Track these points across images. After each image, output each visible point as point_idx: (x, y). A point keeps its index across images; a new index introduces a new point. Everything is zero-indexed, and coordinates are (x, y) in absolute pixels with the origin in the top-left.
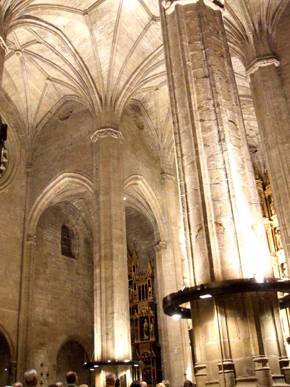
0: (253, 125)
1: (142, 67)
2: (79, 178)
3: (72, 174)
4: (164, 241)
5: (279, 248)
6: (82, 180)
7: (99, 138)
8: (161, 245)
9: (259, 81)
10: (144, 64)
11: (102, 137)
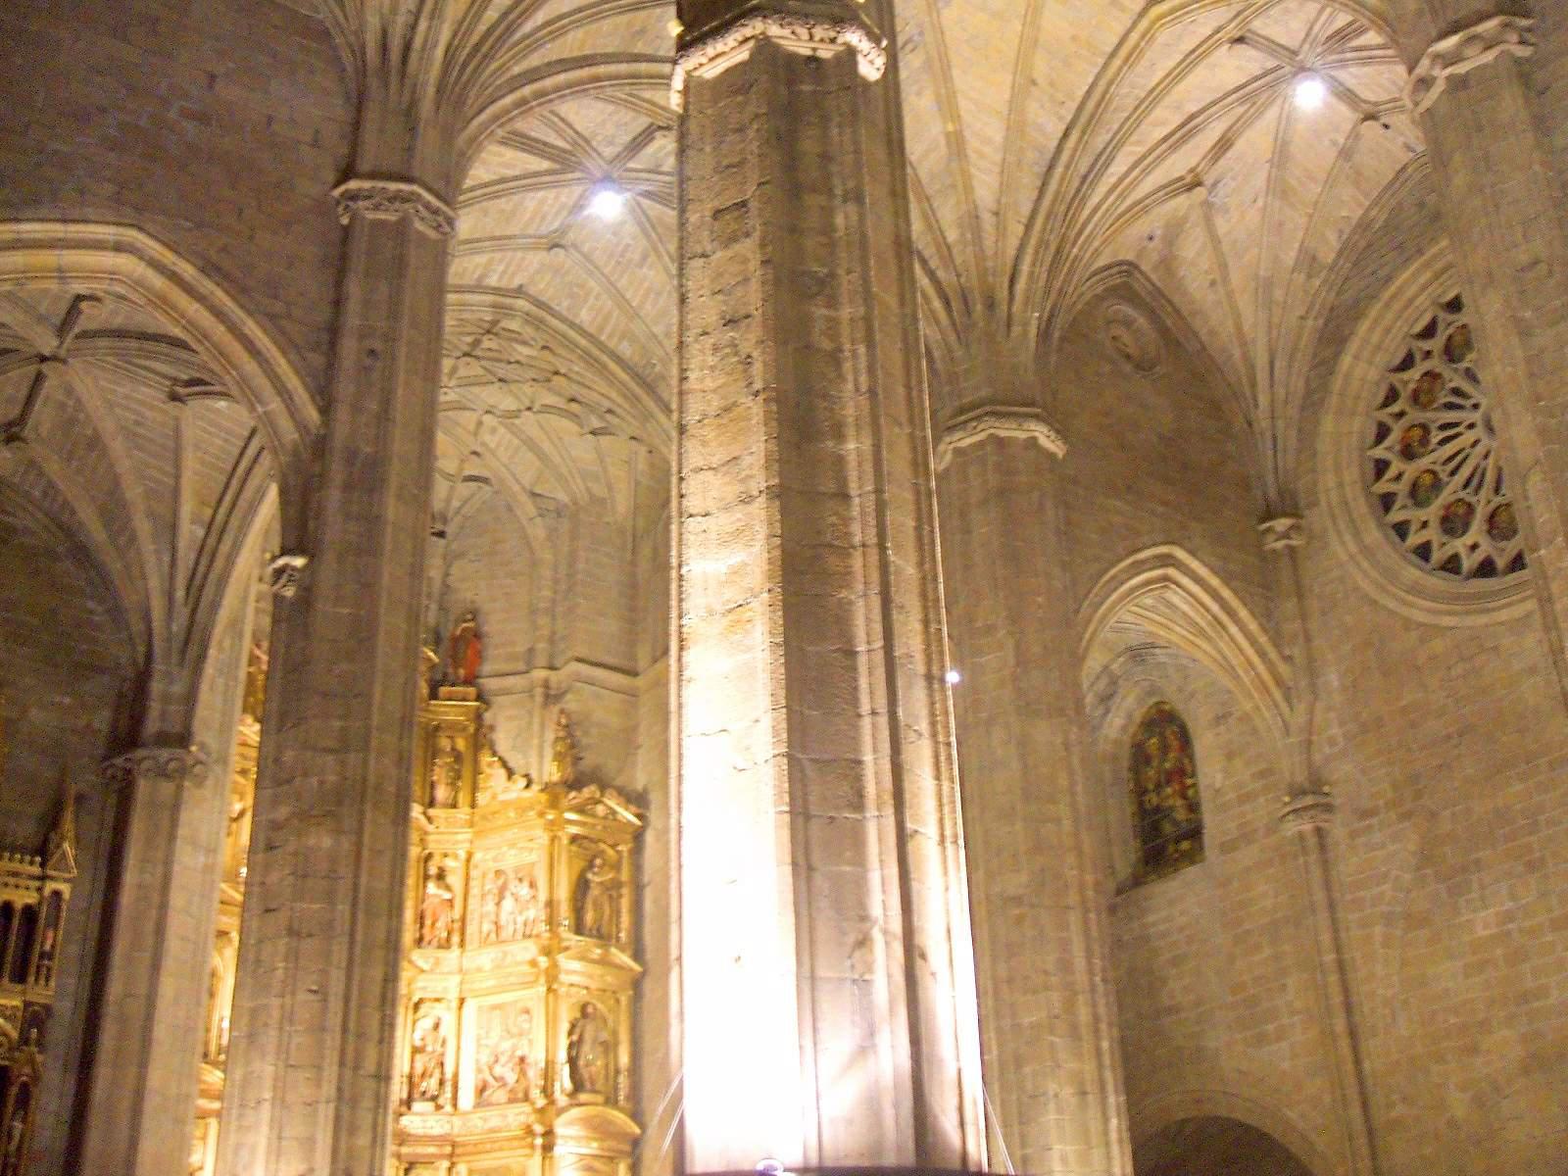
0: (492, 445)
1: (602, 70)
2: (219, 314)
3: (187, 270)
4: (202, 746)
5: (427, 939)
6: (235, 330)
7: (404, 223)
8: (190, 761)
9: (1024, 479)
10: (613, 68)
11: (419, 226)
